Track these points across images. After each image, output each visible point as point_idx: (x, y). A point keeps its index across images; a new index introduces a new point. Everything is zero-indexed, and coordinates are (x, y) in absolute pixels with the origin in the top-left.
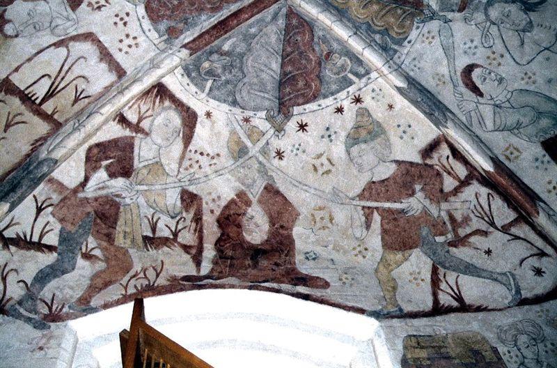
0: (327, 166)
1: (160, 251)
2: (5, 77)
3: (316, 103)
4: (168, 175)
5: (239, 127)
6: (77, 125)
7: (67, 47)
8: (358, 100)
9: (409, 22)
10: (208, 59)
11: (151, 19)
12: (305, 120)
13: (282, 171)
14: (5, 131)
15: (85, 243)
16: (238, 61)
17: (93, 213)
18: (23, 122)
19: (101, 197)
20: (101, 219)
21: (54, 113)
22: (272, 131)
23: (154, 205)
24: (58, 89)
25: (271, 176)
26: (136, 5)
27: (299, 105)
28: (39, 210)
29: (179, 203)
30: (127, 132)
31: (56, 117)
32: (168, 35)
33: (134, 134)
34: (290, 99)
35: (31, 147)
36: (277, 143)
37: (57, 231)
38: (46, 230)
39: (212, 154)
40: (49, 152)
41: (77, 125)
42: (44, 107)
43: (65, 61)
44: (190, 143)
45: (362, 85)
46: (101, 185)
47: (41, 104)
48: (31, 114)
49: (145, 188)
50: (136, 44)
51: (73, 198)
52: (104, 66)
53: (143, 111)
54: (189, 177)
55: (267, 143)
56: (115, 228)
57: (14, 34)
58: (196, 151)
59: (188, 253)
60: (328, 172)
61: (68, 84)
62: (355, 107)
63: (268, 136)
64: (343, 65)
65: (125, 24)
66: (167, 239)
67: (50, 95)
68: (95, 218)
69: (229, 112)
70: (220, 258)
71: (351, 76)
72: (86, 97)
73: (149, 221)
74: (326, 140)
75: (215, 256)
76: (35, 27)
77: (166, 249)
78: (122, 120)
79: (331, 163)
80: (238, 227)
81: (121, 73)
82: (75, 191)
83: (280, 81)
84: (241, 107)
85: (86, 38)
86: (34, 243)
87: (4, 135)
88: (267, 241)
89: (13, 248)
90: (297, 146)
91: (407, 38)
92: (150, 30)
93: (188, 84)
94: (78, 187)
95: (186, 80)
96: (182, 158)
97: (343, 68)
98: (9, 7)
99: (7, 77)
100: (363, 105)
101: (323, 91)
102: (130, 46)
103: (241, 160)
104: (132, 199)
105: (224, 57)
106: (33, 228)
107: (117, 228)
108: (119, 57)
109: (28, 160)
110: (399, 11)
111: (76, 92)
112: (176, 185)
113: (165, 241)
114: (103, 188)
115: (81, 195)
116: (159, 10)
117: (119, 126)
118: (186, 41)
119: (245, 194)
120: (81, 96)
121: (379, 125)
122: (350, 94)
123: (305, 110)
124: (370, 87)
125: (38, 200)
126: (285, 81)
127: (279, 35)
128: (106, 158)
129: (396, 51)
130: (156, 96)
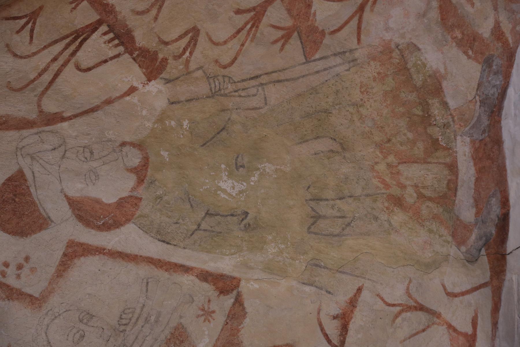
2: (153, 82)
7: (41, 112)
24: (67, 41)
42: (94, 17)
43: (47, 89)
47: (99, 23)
48: (118, 9)
57: (126, 149)
61: (45, 47)
76: (92, 153)
85: (5, 122)
98: (125, 194)
99: (149, 80)
111: (32, 31)
120: (24, 20)
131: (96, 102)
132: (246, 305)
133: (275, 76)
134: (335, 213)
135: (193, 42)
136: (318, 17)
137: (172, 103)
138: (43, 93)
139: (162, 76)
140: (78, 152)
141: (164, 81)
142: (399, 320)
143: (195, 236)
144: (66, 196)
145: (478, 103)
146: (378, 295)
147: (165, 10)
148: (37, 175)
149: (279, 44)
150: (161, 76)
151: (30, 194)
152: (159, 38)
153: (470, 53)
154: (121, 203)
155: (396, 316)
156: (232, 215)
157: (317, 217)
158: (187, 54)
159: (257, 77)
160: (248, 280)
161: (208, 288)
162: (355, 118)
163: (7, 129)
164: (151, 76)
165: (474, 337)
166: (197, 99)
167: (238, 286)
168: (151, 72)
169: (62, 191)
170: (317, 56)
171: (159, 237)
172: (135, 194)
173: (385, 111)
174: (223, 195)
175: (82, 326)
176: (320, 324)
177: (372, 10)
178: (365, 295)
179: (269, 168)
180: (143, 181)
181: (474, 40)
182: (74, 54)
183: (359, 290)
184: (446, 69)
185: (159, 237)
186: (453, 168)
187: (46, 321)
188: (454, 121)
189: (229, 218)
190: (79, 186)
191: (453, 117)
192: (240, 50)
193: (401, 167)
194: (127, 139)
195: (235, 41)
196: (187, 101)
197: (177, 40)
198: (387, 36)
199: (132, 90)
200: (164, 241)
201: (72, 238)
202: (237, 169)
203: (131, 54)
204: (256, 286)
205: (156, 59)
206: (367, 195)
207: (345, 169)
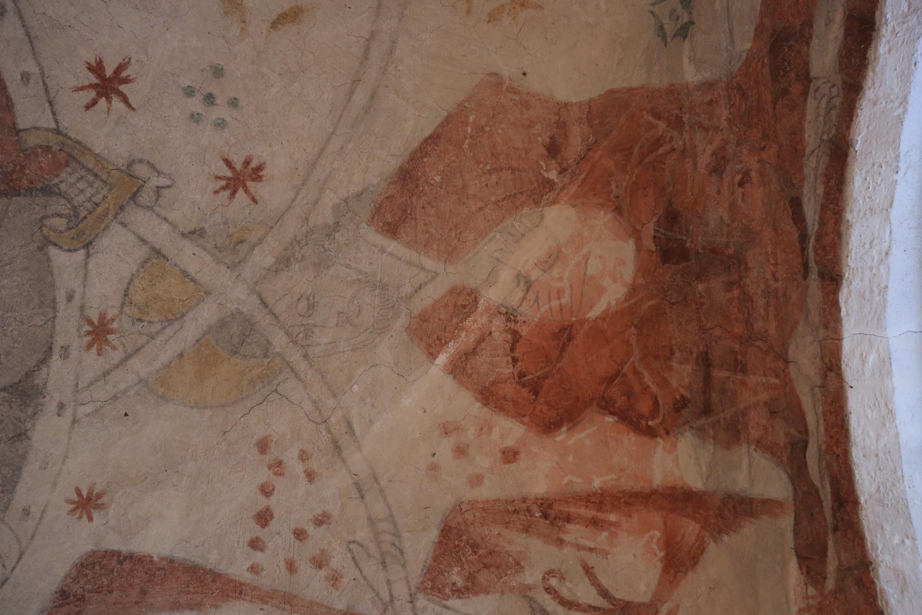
5: (135, 363)
13: (313, 165)
25: (336, 208)
39: (265, 475)
44: (217, 576)
54: (370, 568)
55: (196, 234)
58: (255, 544)
59: (695, 558)
63: (160, 235)
69: (68, 413)
70: (707, 410)
75: (701, 432)
80: (570, 338)
84: (44, 361)
88: (618, 210)
90: (196, 104)
103: (279, 341)
119: (424, 318)
123: (25, 77)
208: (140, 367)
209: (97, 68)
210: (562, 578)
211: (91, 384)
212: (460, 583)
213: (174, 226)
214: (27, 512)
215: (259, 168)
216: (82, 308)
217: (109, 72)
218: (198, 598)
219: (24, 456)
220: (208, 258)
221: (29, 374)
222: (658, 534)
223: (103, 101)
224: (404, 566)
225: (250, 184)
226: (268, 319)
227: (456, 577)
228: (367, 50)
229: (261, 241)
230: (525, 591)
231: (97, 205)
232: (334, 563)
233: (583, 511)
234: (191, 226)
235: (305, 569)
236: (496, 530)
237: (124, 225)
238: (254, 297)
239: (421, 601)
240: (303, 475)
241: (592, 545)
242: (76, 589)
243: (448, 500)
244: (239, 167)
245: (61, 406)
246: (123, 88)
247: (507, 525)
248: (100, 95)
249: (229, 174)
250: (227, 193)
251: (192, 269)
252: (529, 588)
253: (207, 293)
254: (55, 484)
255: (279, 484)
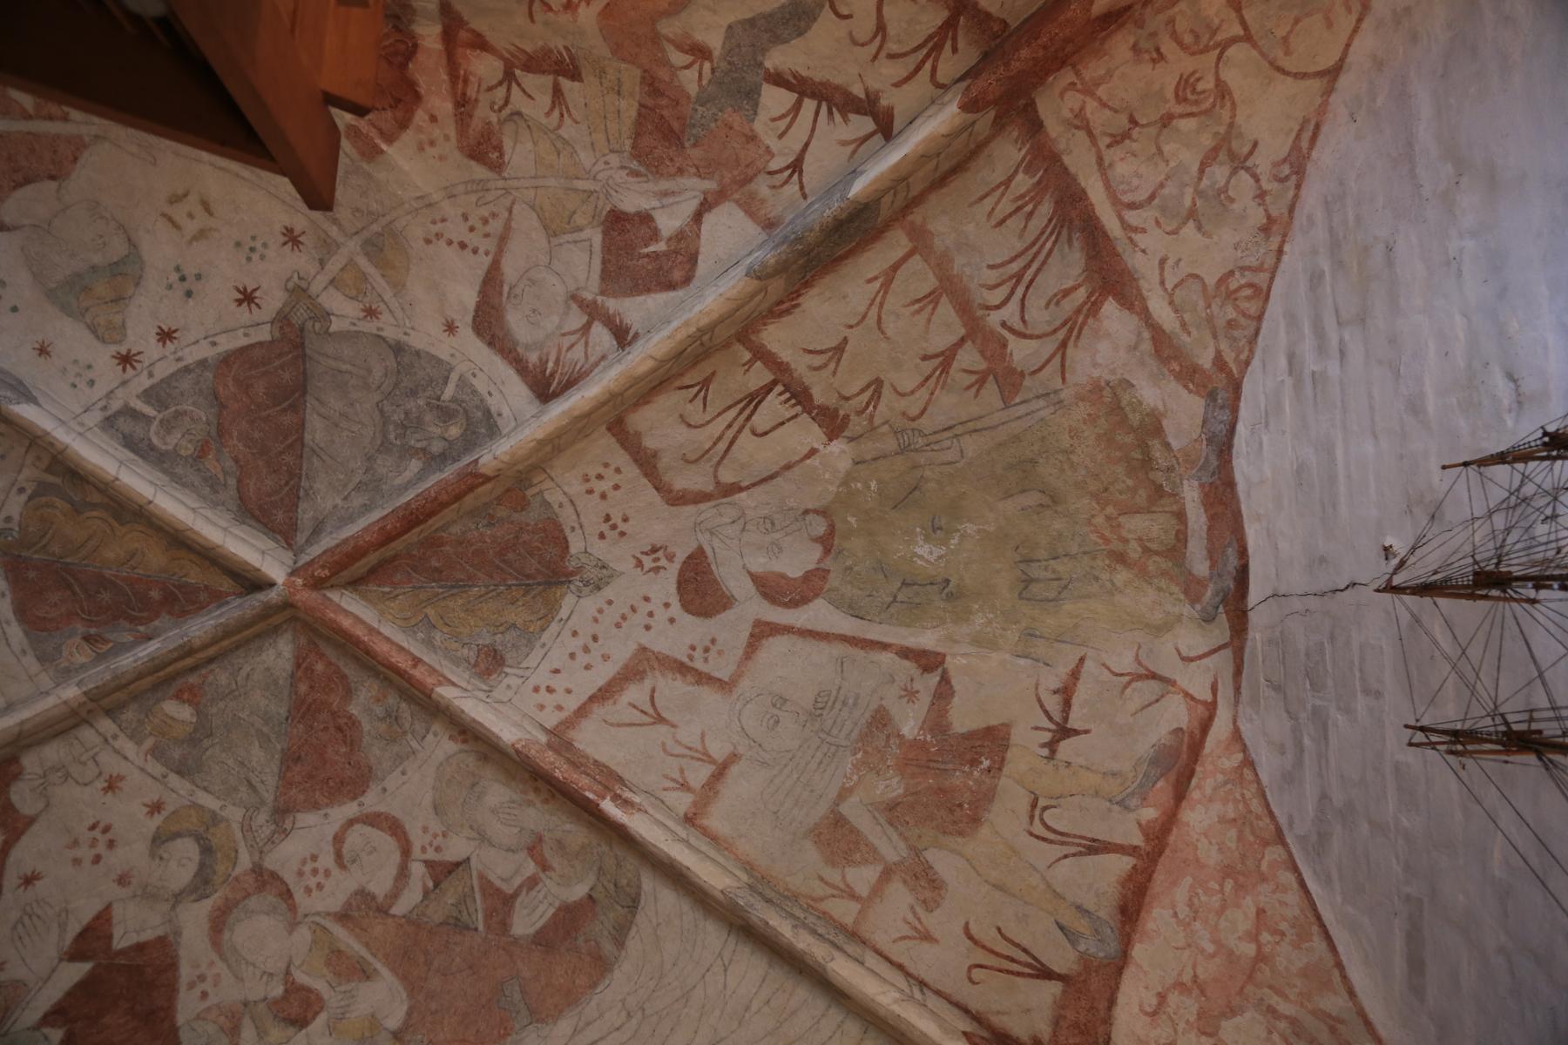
0: (179, 212)
1: (540, 43)
2: (835, 442)
3: (220, 349)
4: (533, 208)
6: (706, 338)
7: (718, 483)
8: (126, 360)
9: (31, 529)
10: (451, 443)
11: (558, 527)
12: (243, 314)
13: (284, 202)
14: (845, 340)
15: (704, 82)
16: (392, 436)
17: (687, 144)
18: (810, 352)
19: (671, 176)
20: (672, 131)
21: (750, 363)
22: (315, 288)
23: (559, 145)
26: (586, 552)
27: (261, 344)
28: (796, 166)
29: (507, 144)
30: (612, 304)
31: (747, 356)
32: (524, 497)
33: (599, 299)
34: (280, 355)
35: (801, 300)
36: (301, 262)
37: (763, 117)
38: (789, 119)
39: (442, 243)
40: (764, 289)
41: (706, 338)
42: (768, 377)
43: (723, 458)
44: (489, 272)
45: (120, 393)
46: (671, 200)
47: (774, 383)
48: (793, 366)
49: (580, 184)
50: (588, 481)
51: (727, 180)
52: (650, 443)
53: (580, 348)
54: (490, 197)
55: (322, 263)
56: (642, 105)
57: (810, 517)
58: (475, 251)
59: (478, 35)
60: (175, 199)
61: (719, 414)
62: (132, 343)
64: (169, 431)
65: (608, 518)
66: (527, 68)
67: (754, 399)
68: (683, 132)
69: (408, 331)
71: (148, 410)
72: (688, 387)
73: (568, 111)
74: (190, 271)
75: (411, 22)
76: (773, 524)
77: (529, 48)
78: (623, 336)
79: (170, 220)
81: (618, 428)
82: (721, 196)
83: (304, 393)
84: (384, 339)
86: (813, 96)
87: (847, 332)
89: (858, 90)
90: (255, 257)
91: (30, 498)
92: (561, 505)
93: (490, 394)
94: (716, 203)
95: (493, 403)
96: (503, 239)
97: (167, 426)
98: (811, 567)
100: (113, 349)
101: (209, 375)
102: (600, 477)
103: (375, 228)
104: (607, 163)
105: (419, 445)
106: (813, 130)
107: (636, 105)
108: (621, 458)
109: (808, 277)
110: (56, 549)
111: (705, 398)
112: (515, 183)
113: (534, 63)
114: (665, 194)
115: (710, 185)
116: (542, 543)
117: (627, 321)
118: (489, 486)
119: (363, 154)
120: (697, 388)
121: (65, 309)
122: (145, 372)
123: (246, 335)
124: (100, 391)
125: (797, 187)
126: (293, 395)
127: (311, 487)
128: (656, 256)
129: (48, 470)
130: (552, 375)
131: (775, 468)
132: (954, 682)
133: (971, 425)
134: (1049, 575)
135: (877, 395)
136: (1016, 358)
137: (857, 463)
138: (719, 463)
139: (845, 434)
140: (758, 523)
141: (846, 440)
142: (1128, 691)
143: (892, 610)
144: (749, 572)
145: (1205, 442)
146: (1104, 665)
147: (843, 363)
148: (717, 550)
149: (974, 390)
150: (844, 434)
151: (711, 572)
152: (839, 393)
153: (1191, 386)
154: (807, 577)
155: (1126, 687)
156: (931, 584)
157: (1029, 581)
158: (871, 408)
159: (950, 428)
160: (954, 655)
161: (909, 666)
162: (1066, 466)
163: (685, 504)
164: (832, 436)
165: (1215, 703)
166: (885, 457)
167: (943, 662)
168: (832, 431)
169: (744, 567)
170: (1017, 400)
171: (851, 612)
172: (822, 565)
173: (1100, 457)
174: (919, 562)
175: (775, 711)
176: (1039, 700)
177: (1076, 346)
178: (1089, 665)
179: (970, 528)
180: (830, 551)
181: (1194, 372)
182: (749, 418)
183: (1082, 660)
184: (1165, 406)
185: (851, 612)
186: (1181, 516)
187: (737, 708)
188: (1179, 464)
189: (929, 587)
190: (762, 560)
191: (1177, 459)
192: (930, 400)
193: (1122, 519)
194: (810, 506)
195: (923, 390)
196: (874, 459)
197: (858, 394)
198: (1096, 373)
199: (813, 452)
200: (857, 617)
201: (759, 617)
202: (934, 531)
203: (809, 413)
204: (964, 662)
205: (837, 416)
206: (1085, 553)
207: (1058, 525)
208: (388, 296)
209: (240, 302)
210: (494, 103)
211: (395, 318)
212: (497, 154)
213: (318, 273)
214: (452, 355)
215: (286, 228)
216: (359, 319)
217: (241, 296)
218: (498, 282)
219: (427, 353)
220: (334, 258)
221: (390, 346)
222: (468, 52)
223: (256, 300)
224: (489, 180)
225: (295, 234)
226: (365, 232)
227: (494, 156)
228: (221, 169)
229: (325, 232)
230: (501, 123)
231: (308, 308)
232: (486, 214)
233: (460, 86)
234: (318, 265)
235: (488, 229)
236: (471, 132)
237: (318, 296)
238: (355, 237)
239: (505, 175)
240: (444, 224)
241: (477, 85)
242: (488, 338)
243: (457, 155)
244: (286, 239)
245: (406, 334)
246: (249, 291)
247: (468, 126)
248: (253, 302)
249: (290, 244)
250: (301, 246)
251: (341, 266)
252: (499, 120)
253: (352, 260)
254: (441, 341)
255: (447, 236)
